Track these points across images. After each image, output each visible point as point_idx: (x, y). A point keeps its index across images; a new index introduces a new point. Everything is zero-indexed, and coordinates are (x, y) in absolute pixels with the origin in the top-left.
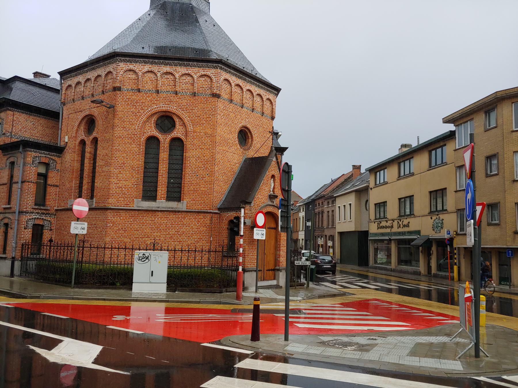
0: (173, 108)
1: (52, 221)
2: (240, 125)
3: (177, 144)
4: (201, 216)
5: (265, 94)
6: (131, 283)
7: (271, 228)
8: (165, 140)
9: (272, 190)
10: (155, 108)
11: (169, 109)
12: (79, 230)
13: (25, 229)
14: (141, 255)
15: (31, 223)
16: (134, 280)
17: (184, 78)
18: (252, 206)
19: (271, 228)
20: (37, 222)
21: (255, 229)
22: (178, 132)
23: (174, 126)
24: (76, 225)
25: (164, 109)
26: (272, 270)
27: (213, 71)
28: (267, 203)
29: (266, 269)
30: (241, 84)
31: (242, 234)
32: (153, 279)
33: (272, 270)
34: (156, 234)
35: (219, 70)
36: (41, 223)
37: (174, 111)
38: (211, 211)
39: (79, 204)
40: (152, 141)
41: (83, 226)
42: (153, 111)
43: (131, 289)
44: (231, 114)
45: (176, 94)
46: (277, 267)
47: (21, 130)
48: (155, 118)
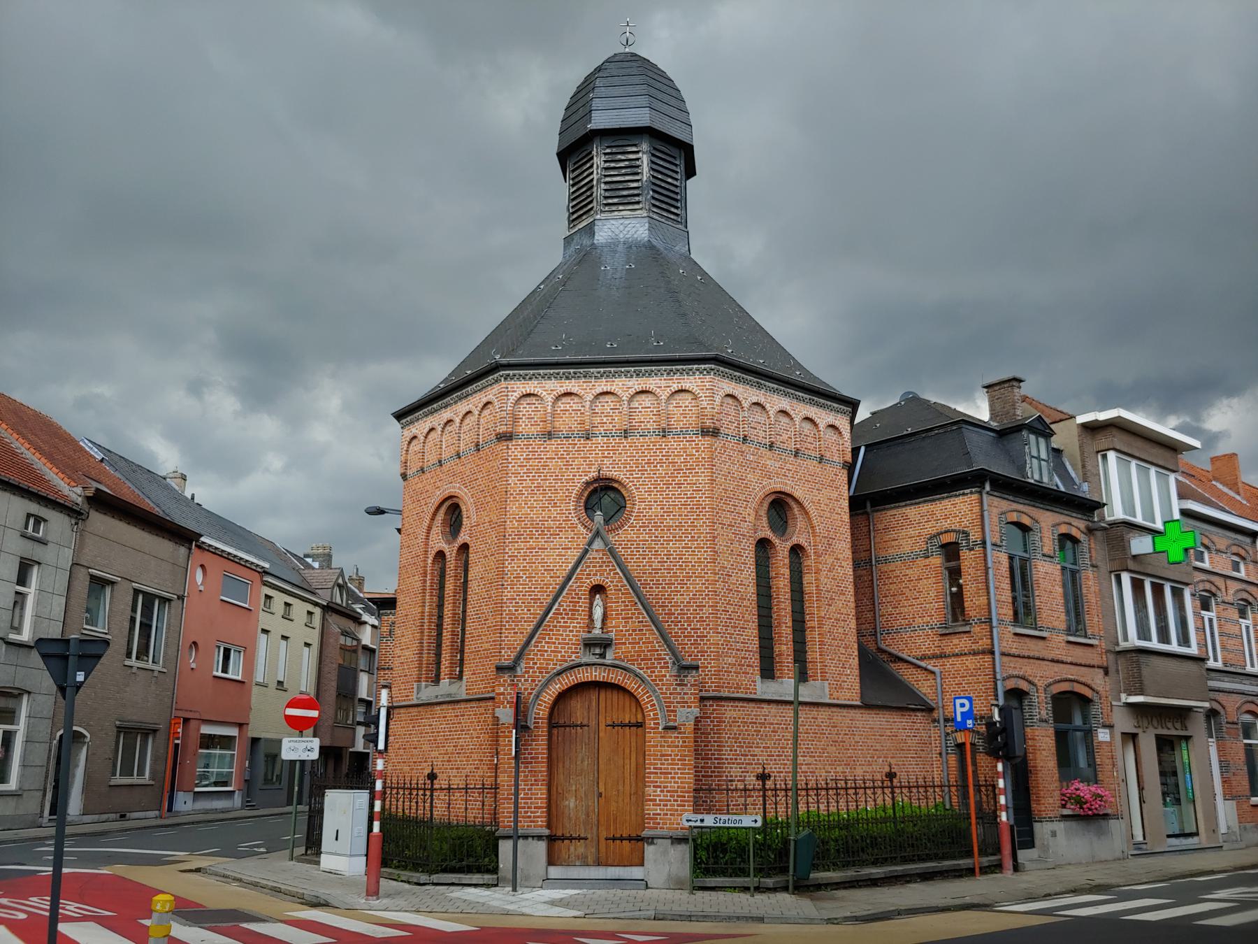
0: (456, 488)
2: (585, 479)
5: (663, 383)
6: (319, 853)
7: (623, 725)
8: (451, 551)
9: (598, 624)
12: (300, 752)
17: (467, 421)
18: (519, 673)
19: (623, 725)
26: (630, 839)
27: (496, 388)
28: (578, 661)
29: (604, 834)
30: (575, 390)
31: (381, 746)
33: (630, 839)
35: (503, 384)
41: (309, 745)
42: (436, 504)
43: (318, 863)
46: (646, 833)
48: (441, 516)
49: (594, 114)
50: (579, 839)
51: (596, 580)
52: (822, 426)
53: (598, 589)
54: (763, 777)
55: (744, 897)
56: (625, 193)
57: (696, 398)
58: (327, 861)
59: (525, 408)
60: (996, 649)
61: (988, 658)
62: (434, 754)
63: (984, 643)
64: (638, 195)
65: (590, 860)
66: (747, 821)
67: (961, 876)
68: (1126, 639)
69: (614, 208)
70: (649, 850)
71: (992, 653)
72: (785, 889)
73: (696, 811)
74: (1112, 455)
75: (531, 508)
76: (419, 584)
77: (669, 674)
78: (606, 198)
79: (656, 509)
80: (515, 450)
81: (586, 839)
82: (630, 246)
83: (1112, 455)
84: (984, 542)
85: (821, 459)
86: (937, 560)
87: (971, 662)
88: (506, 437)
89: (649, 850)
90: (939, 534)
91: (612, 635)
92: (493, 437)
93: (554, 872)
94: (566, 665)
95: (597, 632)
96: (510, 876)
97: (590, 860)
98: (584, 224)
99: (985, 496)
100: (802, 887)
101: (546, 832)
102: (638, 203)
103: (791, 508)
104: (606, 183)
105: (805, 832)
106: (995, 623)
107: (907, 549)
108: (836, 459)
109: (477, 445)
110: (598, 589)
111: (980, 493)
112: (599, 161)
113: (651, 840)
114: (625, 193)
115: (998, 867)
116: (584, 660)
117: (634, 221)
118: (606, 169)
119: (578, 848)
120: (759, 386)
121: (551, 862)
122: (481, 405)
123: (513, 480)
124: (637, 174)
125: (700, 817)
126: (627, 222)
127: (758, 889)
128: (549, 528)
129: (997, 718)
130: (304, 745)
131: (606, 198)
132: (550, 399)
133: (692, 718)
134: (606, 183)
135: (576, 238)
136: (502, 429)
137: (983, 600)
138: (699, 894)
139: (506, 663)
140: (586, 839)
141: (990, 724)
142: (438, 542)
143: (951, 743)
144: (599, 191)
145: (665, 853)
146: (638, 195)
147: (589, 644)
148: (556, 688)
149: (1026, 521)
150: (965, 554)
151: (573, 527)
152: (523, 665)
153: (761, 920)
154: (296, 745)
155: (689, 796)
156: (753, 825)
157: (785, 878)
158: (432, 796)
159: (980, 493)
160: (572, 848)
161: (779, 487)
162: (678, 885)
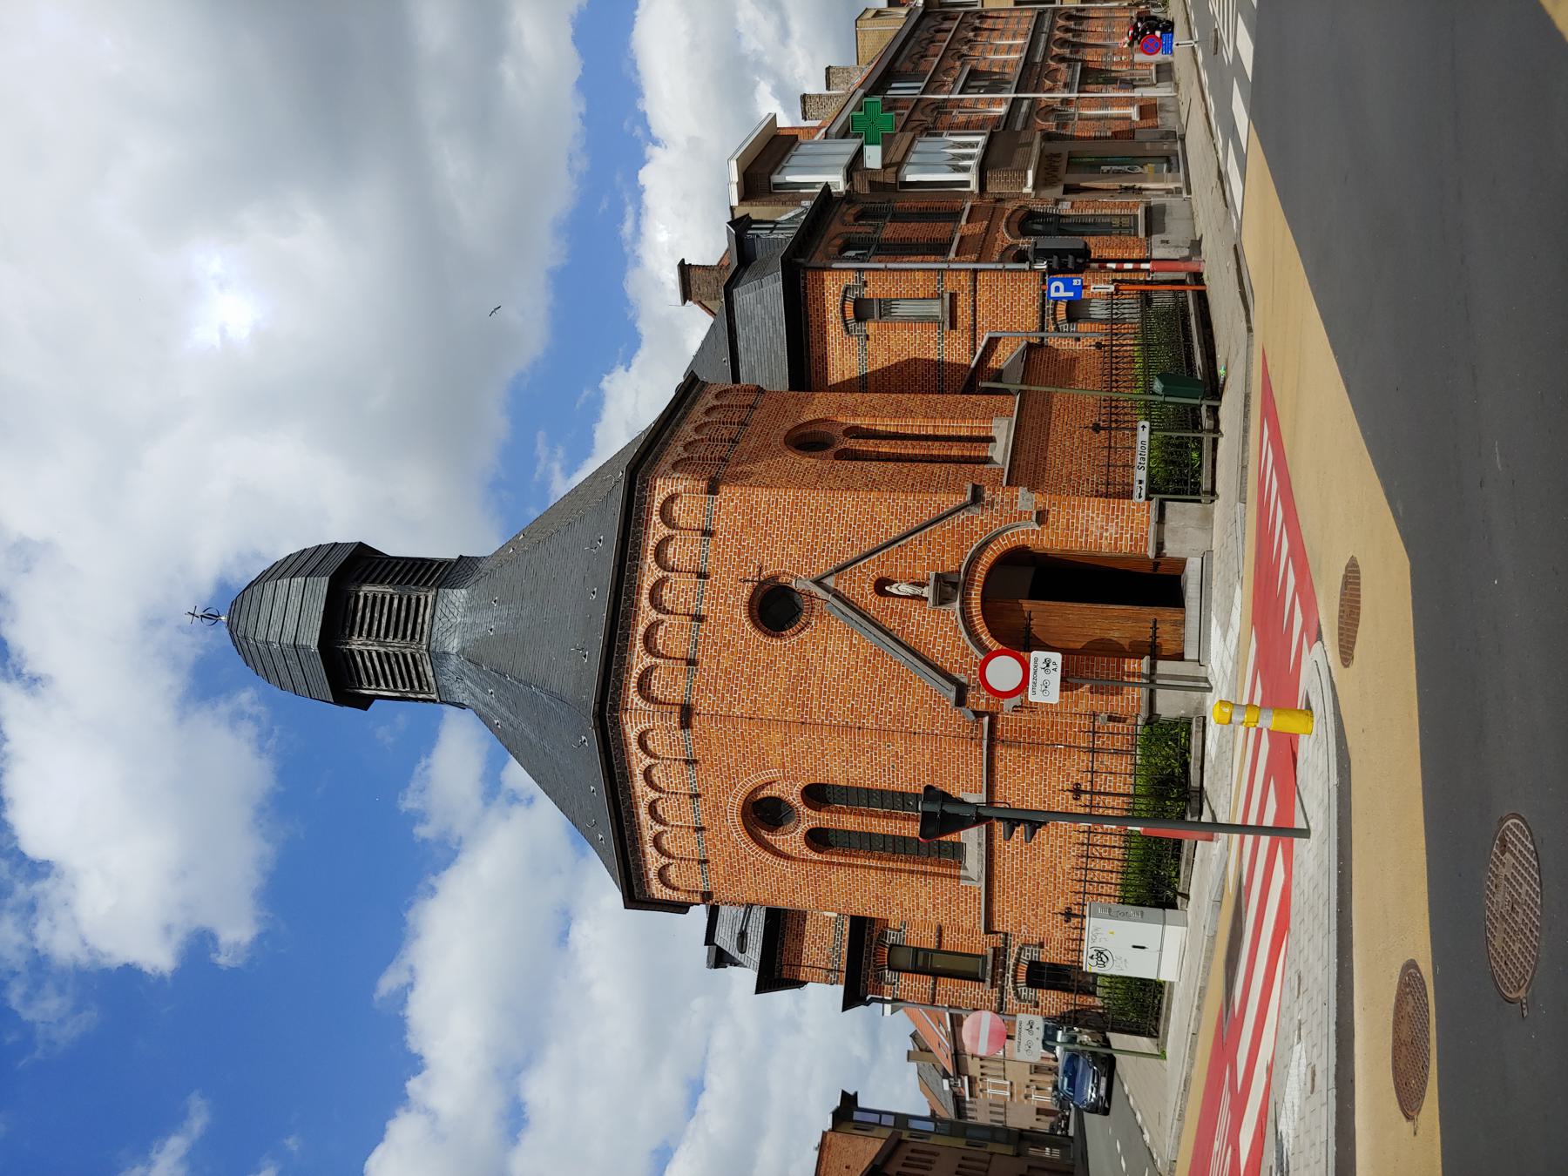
1: (1020, 941)
2: (748, 626)
3: (817, 795)
4: (999, 765)
9: (918, 591)
10: (739, 835)
11: (737, 810)
13: (1037, 1005)
14: (1094, 962)
15: (1025, 992)
16: (1153, 977)
20: (1022, 977)
21: (1031, 698)
22: (792, 794)
23: (777, 802)
24: (1023, 1047)
25: (738, 820)
28: (958, 613)
32: (1153, 946)
34: (1047, 853)
36: (1024, 967)
37: (739, 801)
38: (985, 743)
39: (976, 1039)
40: (818, 839)
41: (1025, 1026)
43: (1171, 984)
44: (725, 664)
45: (698, 796)
46: (1151, 554)
47: (820, 949)
49: (302, 641)
50: (1155, 628)
51: (869, 588)
52: (716, 403)
53: (881, 586)
54: (1096, 428)
55: (1222, 442)
56: (403, 614)
57: (672, 498)
58: (1167, 974)
59: (656, 688)
60: (972, 266)
61: (980, 276)
62: (1047, 853)
63: (965, 280)
64: (409, 600)
65: (1179, 617)
66: (1143, 435)
67: (1206, 301)
68: (966, 184)
69: (419, 628)
70: (1171, 550)
71: (975, 271)
72: (1214, 411)
73: (1129, 495)
74: (776, 179)
75: (774, 690)
76: (842, 873)
77: (979, 516)
78: (404, 637)
79: (792, 549)
80: (703, 705)
81: (1155, 622)
82: (471, 609)
83: (776, 179)
84: (859, 270)
85: (752, 407)
86: (871, 327)
87: (983, 296)
88: (687, 715)
89: (1171, 550)
90: (845, 321)
91: (932, 574)
92: (679, 733)
93: (1191, 653)
94: (961, 627)
95: (927, 592)
96: (1196, 695)
97: (1179, 617)
98: (428, 669)
99: (812, 264)
100: (1214, 389)
101: (1146, 661)
102: (418, 599)
103: (804, 435)
104: (386, 636)
105: (1158, 386)
106: (945, 266)
107: (855, 360)
108: (753, 397)
109: (687, 762)
110: (881, 586)
111: (806, 269)
112: (356, 644)
113: (1160, 546)
114: (403, 614)
115: (1197, 277)
116: (957, 605)
117: (439, 605)
118: (369, 634)
119: (1165, 630)
120: (666, 443)
121: (1180, 657)
122: (640, 754)
123: (737, 711)
124: (383, 598)
125: (1137, 484)
126: (438, 613)
127: (1216, 429)
128: (799, 670)
129: (1043, 266)
130: (1025, 1033)
131: (404, 637)
132: (649, 660)
133: (1028, 495)
134: (386, 636)
135: (443, 680)
136: (675, 721)
137: (919, 275)
138: (1219, 489)
139: (953, 695)
140: (1155, 622)
141: (1051, 271)
142: (791, 839)
143: (1064, 326)
144: (394, 645)
145: (1174, 531)
146: (409, 600)
147: (942, 599)
148: (985, 637)
149: (839, 242)
150: (867, 293)
151: (802, 642)
152: (957, 675)
153: (1247, 397)
154: (1023, 1042)
155: (1114, 503)
156: (1147, 430)
157: (1204, 409)
158: (1100, 793)
159: (806, 269)
160: (1166, 637)
161: (780, 439)
162: (1208, 519)
